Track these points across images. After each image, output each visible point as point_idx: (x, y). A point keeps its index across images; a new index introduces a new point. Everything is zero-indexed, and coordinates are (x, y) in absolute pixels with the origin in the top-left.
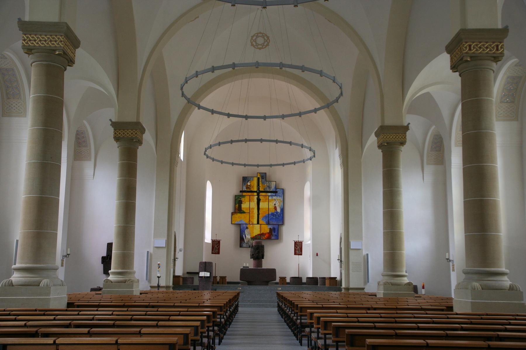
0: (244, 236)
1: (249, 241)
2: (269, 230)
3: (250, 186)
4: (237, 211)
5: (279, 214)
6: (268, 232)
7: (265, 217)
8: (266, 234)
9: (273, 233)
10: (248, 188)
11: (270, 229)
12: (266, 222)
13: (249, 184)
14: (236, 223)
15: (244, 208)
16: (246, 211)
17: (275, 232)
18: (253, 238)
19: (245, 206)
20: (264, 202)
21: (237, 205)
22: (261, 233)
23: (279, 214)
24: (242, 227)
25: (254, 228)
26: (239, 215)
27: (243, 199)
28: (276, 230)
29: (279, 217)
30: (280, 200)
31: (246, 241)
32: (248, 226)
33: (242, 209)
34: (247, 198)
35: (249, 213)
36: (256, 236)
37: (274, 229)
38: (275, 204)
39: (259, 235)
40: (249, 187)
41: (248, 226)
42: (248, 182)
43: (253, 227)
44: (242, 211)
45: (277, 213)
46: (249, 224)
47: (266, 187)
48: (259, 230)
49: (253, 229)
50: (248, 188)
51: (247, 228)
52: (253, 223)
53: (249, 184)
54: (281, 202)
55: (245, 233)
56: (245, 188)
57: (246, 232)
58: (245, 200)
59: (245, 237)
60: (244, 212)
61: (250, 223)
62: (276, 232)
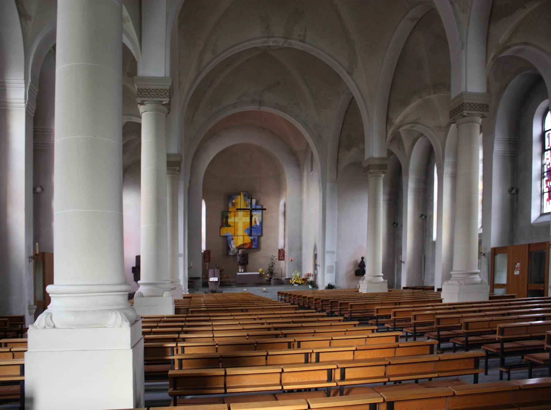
0: (230, 246)
1: (234, 250)
2: (250, 240)
3: (235, 203)
4: (224, 225)
5: (258, 227)
6: (250, 242)
7: (247, 229)
8: (247, 244)
9: (254, 243)
10: (233, 205)
11: (251, 239)
12: (248, 234)
13: (234, 201)
14: (224, 235)
15: (230, 222)
16: (231, 225)
17: (255, 242)
18: (239, 248)
19: (231, 220)
20: (246, 217)
21: (224, 220)
22: (244, 243)
23: (258, 227)
24: (228, 239)
25: (238, 239)
26: (226, 228)
27: (229, 215)
28: (256, 240)
29: (258, 229)
30: (259, 215)
31: (232, 250)
32: (233, 237)
33: (229, 223)
34: (232, 214)
35: (234, 226)
36: (240, 246)
37: (254, 239)
38: (255, 219)
39: (242, 245)
40: (234, 204)
41: (233, 237)
42: (233, 200)
43: (238, 238)
44: (228, 225)
45: (257, 226)
46: (234, 236)
47: (248, 204)
48: (242, 240)
49: (238, 240)
50: (233, 205)
51: (233, 239)
52: (237, 234)
53: (234, 201)
54: (260, 216)
55: (231, 243)
56: (231, 205)
57: (232, 242)
58: (231, 215)
59: (231, 246)
60: (230, 226)
61: (235, 235)
62: (256, 242)
